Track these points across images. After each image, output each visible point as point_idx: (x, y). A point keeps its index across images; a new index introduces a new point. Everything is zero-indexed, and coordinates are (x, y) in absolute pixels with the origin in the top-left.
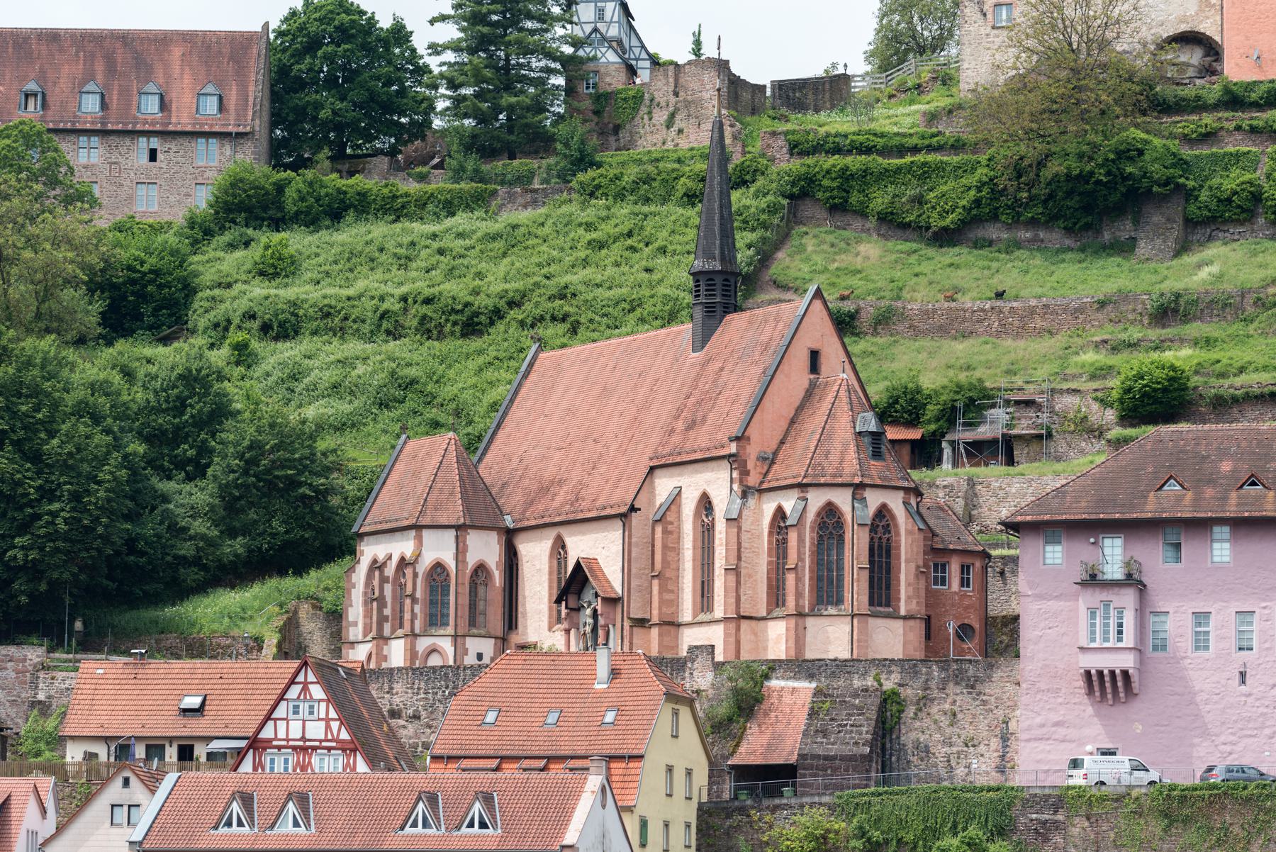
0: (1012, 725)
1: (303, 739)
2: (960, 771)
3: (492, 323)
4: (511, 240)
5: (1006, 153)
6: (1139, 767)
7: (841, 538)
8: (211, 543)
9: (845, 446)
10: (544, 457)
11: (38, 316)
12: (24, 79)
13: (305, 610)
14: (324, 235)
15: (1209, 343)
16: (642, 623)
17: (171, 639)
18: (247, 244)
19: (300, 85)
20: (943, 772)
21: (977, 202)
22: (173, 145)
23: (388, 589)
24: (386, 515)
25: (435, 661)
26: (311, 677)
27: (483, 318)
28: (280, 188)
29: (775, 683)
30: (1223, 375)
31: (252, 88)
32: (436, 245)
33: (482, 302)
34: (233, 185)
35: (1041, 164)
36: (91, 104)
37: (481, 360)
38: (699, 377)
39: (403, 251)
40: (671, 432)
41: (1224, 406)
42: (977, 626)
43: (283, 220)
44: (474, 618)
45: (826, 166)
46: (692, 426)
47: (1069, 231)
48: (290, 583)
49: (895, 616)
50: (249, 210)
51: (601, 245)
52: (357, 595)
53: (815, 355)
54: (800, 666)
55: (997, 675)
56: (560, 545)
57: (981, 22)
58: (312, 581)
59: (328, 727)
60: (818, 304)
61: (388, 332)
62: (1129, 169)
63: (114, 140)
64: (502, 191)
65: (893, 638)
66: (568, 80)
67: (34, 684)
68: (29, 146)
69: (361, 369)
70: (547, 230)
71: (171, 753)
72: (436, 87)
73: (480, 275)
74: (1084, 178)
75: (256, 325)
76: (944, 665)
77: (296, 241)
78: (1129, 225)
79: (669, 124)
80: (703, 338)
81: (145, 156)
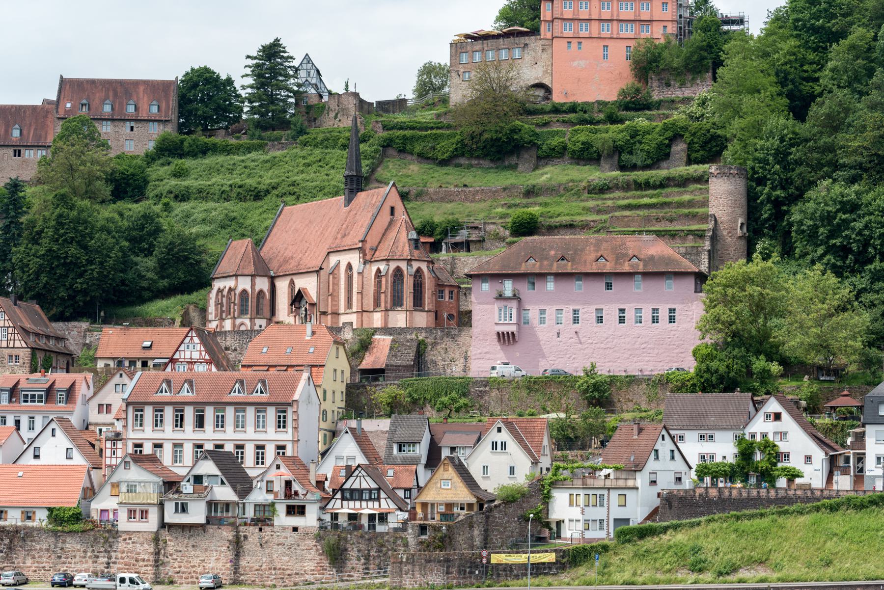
0: (469, 353)
2: (449, 371)
3: (266, 195)
4: (273, 163)
5: (468, 130)
6: (518, 370)
7: (402, 281)
8: (155, 282)
9: (404, 244)
11: (87, 192)
12: (81, 99)
13: (191, 308)
14: (199, 161)
15: (546, 205)
16: (324, 313)
17: (139, 319)
18: (169, 164)
19: (191, 101)
20: (442, 371)
21: (456, 149)
22: (140, 125)
23: (224, 300)
24: (224, 271)
25: (243, 328)
26: (194, 334)
27: (262, 193)
28: (182, 142)
29: (376, 337)
30: (551, 217)
31: (171, 102)
32: (243, 164)
33: (262, 187)
34: (163, 141)
35: (481, 134)
36: (107, 108)
37: (261, 210)
38: (347, 217)
39: (230, 167)
40: (336, 238)
41: (552, 229)
42: (455, 314)
43: (183, 154)
44: (258, 312)
46: (344, 236)
47: (492, 161)
48: (186, 297)
50: (170, 150)
51: (309, 165)
52: (212, 302)
53: (392, 209)
54: (386, 330)
55: (463, 334)
56: (292, 283)
58: (194, 296)
60: (394, 189)
61: (225, 199)
62: (516, 137)
63: (117, 123)
64: (270, 143)
65: (422, 319)
66: (296, 100)
67: (85, 337)
68: (83, 124)
69: (214, 213)
70: (287, 159)
71: (139, 364)
72: (243, 102)
73: (261, 176)
74: (498, 140)
75: (172, 196)
76: (442, 330)
77: (188, 163)
78: (515, 158)
79: (336, 118)
80: (348, 202)
81: (129, 129)
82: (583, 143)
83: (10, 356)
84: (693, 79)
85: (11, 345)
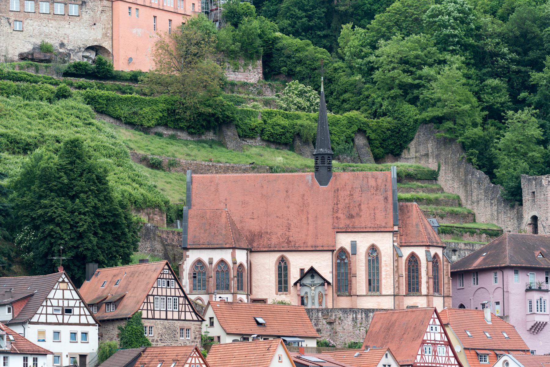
1: (435, 340)
10: (241, 222)
45: (100, 94)
46: (351, 217)
47: (191, 134)
57: (8, 26)
59: (441, 336)
74: (213, 115)
82: (284, 127)
83: (182, 329)
84: (246, 65)
85: (183, 318)
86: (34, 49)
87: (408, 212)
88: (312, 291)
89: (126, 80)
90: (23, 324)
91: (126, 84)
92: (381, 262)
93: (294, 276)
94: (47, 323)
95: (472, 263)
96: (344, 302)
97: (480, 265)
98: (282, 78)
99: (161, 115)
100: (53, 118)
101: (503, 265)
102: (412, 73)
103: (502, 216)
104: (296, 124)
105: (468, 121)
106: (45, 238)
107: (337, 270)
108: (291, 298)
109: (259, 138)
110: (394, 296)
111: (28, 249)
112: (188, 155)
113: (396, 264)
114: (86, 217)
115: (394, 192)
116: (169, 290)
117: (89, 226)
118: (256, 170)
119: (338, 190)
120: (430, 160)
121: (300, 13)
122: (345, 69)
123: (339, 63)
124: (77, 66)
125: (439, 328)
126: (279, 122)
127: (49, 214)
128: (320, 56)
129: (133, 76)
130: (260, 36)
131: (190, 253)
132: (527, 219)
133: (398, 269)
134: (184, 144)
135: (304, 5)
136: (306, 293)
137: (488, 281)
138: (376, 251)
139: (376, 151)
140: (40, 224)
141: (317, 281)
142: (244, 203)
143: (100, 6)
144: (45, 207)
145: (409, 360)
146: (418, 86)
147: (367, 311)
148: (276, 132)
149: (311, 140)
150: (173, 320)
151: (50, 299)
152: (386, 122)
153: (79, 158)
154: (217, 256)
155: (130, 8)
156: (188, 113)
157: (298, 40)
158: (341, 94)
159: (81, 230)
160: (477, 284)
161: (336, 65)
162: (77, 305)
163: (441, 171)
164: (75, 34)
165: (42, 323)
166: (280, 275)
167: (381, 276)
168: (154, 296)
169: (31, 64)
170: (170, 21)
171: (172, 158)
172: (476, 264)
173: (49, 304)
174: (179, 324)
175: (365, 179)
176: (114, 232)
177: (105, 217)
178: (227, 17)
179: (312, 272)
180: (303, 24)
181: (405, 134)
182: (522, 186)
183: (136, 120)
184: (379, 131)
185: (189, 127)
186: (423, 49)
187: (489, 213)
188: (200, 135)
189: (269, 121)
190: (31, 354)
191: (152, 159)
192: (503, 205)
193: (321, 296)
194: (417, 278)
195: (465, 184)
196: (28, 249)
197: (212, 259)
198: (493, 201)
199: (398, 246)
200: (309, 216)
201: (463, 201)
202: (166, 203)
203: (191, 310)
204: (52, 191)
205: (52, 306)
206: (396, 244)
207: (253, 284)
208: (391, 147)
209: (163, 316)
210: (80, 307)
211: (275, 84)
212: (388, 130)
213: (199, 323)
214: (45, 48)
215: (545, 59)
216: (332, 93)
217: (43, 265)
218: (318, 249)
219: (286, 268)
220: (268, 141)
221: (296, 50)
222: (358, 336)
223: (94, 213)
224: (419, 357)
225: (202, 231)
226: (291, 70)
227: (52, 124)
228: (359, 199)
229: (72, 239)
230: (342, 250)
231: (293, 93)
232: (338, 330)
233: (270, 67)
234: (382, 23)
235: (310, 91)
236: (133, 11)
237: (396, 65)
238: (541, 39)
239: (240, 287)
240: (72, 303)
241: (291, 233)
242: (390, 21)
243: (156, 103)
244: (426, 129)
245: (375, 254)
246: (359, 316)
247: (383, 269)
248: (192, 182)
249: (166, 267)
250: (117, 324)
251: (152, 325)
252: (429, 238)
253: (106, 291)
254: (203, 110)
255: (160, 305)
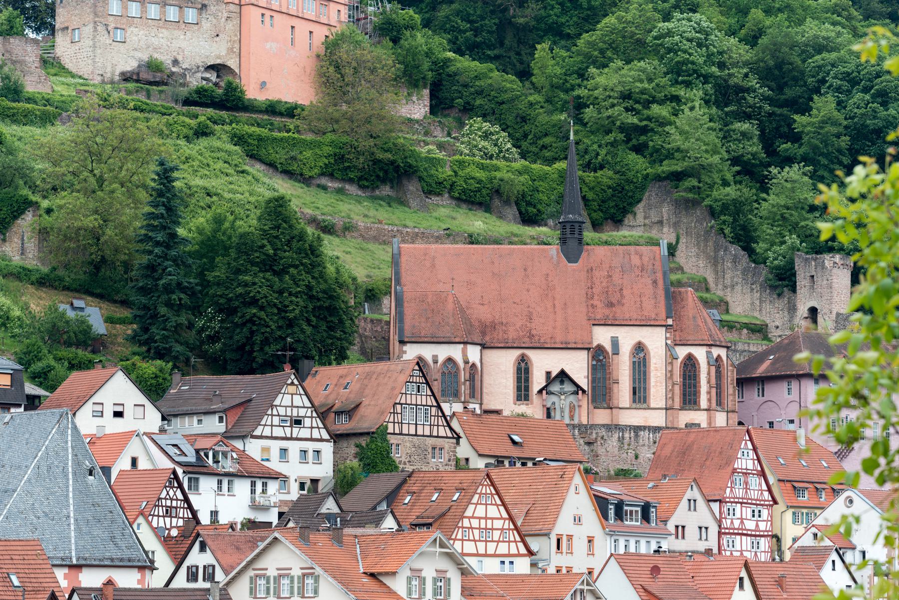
1: (746, 469)
47: (362, 187)
49: (700, 410)
57: (106, 36)
74: (392, 163)
82: (479, 182)
83: (434, 448)
85: (435, 434)
86: (139, 66)
87: (682, 300)
88: (562, 402)
89: (261, 112)
90: (243, 437)
91: (266, 117)
92: (650, 366)
93: (538, 381)
94: (272, 438)
95: (756, 369)
96: (602, 417)
97: (767, 370)
98: (454, 113)
99: (326, 161)
100: (198, 163)
101: (801, 372)
102: (638, 112)
103: (767, 307)
104: (495, 178)
105: (716, 177)
106: (244, 324)
107: (592, 374)
108: (533, 410)
109: (447, 195)
110: (666, 409)
111: (213, 339)
112: (365, 216)
113: (669, 368)
114: (299, 299)
115: (665, 274)
116: (419, 397)
117: (301, 312)
118: (451, 238)
119: (592, 269)
120: (665, 230)
121: (465, 26)
122: (543, 104)
123: (536, 96)
124: (200, 91)
125: (751, 452)
126: (473, 174)
127: (251, 295)
128: (508, 85)
129: (269, 106)
130: (427, 55)
131: (408, 348)
132: (803, 310)
133: (672, 375)
134: (356, 201)
135: (469, 14)
136: (554, 403)
137: (778, 392)
138: (643, 350)
139: (594, 215)
140: (238, 307)
141: (568, 387)
142: (469, 283)
143: (224, 11)
144: (246, 285)
145: (716, 493)
146: (644, 130)
147: (637, 429)
148: (469, 187)
149: (513, 199)
150: (423, 436)
151: (276, 406)
152: (606, 176)
153: (285, 222)
154: (443, 352)
155: (263, 15)
156: (362, 160)
157: (477, 63)
158: (540, 138)
159: (291, 315)
160: (763, 396)
161: (531, 98)
162: (309, 414)
163: (680, 243)
164: (191, 48)
165: (267, 437)
166: (519, 380)
167: (650, 383)
168: (402, 404)
169: (142, 88)
170: (311, 32)
171: (347, 220)
172: (762, 370)
173: (275, 412)
174: (430, 442)
175: (627, 256)
176: (329, 319)
177: (319, 300)
178: (381, 29)
179: (563, 376)
180: (467, 39)
181: (630, 194)
182: (796, 268)
183: (294, 167)
184: (598, 189)
185: (360, 178)
186: (650, 80)
187: (749, 301)
188: (373, 189)
189: (460, 173)
190: (260, 478)
191: (324, 221)
192: (768, 291)
193: (572, 408)
194: (695, 386)
195: (715, 262)
196: (213, 339)
197: (437, 356)
198: (754, 286)
199: (672, 344)
200: (556, 302)
201: (712, 285)
202: (354, 279)
203: (445, 424)
204: (253, 264)
205: (278, 415)
206: (669, 342)
207: (485, 390)
208: (612, 211)
209: (413, 432)
210: (312, 417)
211: (449, 121)
212: (609, 187)
213: (454, 441)
214: (153, 66)
215: (812, 99)
216: (525, 136)
217: (237, 360)
218: (569, 346)
219: (527, 371)
220: (458, 199)
221: (476, 77)
222: (625, 461)
223: (306, 294)
224: (728, 490)
225: (423, 320)
226: (468, 103)
227: (196, 171)
228: (620, 281)
229: (280, 328)
230: (600, 349)
231: (476, 134)
232: (599, 452)
233: (438, 97)
234: (592, 44)
235: (497, 133)
236: (267, 19)
237: (615, 101)
238: (802, 73)
239: (472, 395)
240: (302, 412)
241: (533, 325)
242: (604, 42)
243: (319, 145)
244: (660, 187)
245: (642, 355)
246: (627, 435)
247: (652, 374)
248: (400, 254)
249: (417, 368)
250: (353, 441)
251: (399, 442)
252: (711, 336)
253: (332, 397)
254: (381, 156)
255: (408, 416)
